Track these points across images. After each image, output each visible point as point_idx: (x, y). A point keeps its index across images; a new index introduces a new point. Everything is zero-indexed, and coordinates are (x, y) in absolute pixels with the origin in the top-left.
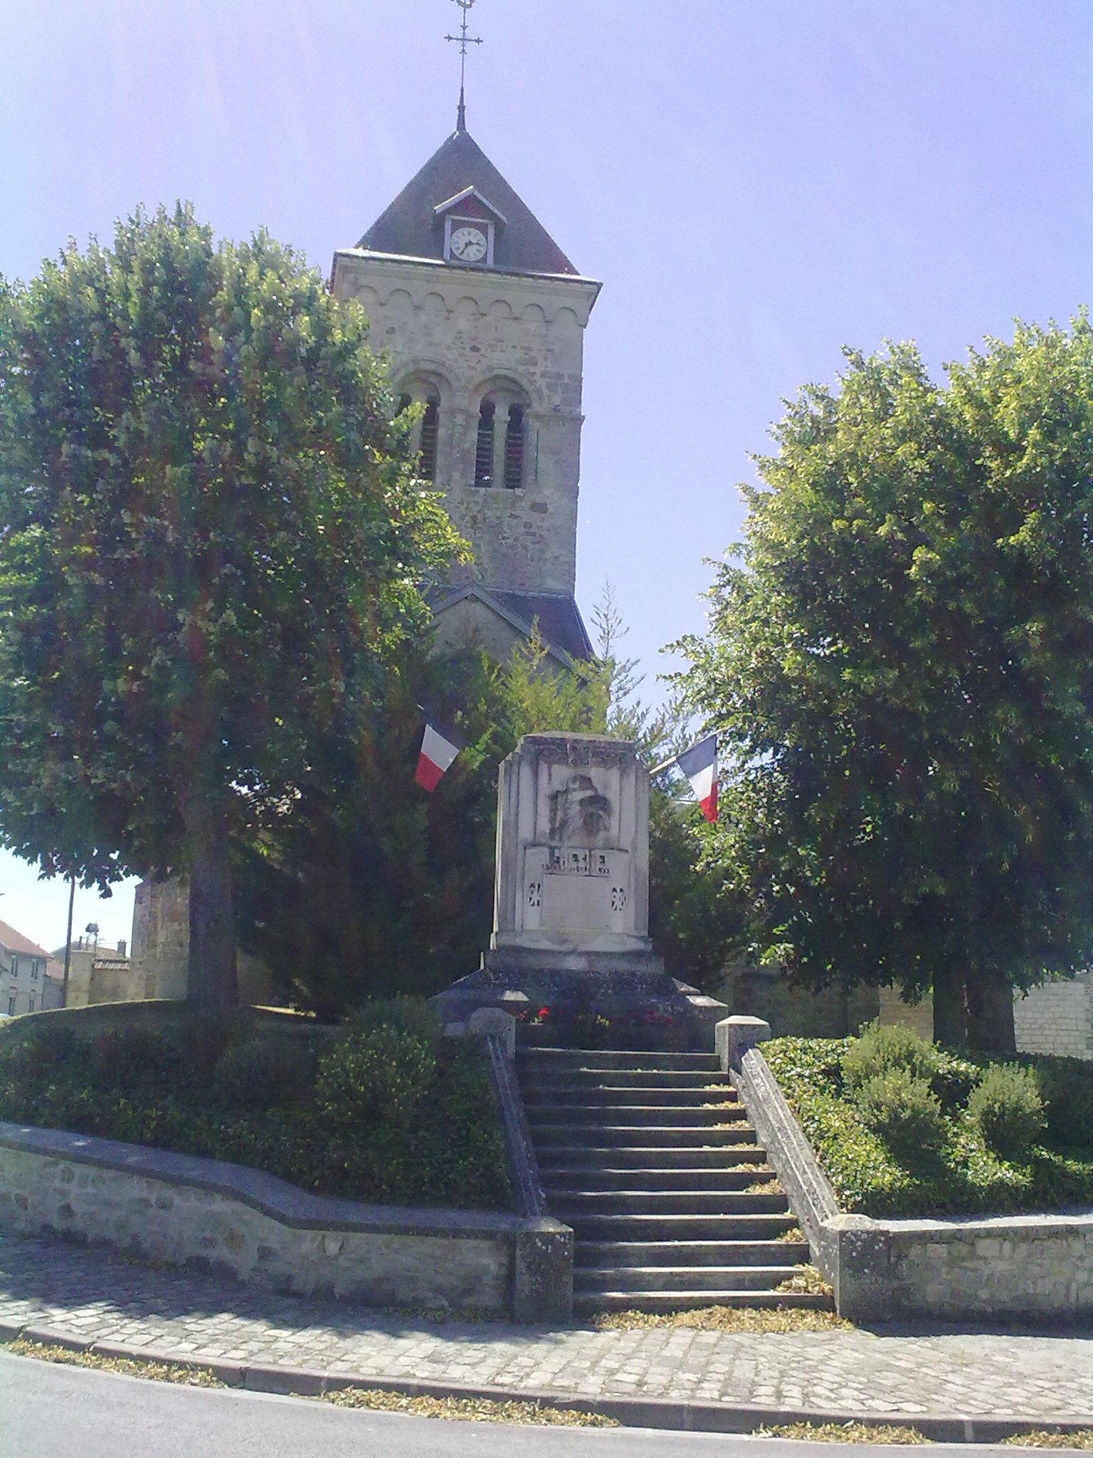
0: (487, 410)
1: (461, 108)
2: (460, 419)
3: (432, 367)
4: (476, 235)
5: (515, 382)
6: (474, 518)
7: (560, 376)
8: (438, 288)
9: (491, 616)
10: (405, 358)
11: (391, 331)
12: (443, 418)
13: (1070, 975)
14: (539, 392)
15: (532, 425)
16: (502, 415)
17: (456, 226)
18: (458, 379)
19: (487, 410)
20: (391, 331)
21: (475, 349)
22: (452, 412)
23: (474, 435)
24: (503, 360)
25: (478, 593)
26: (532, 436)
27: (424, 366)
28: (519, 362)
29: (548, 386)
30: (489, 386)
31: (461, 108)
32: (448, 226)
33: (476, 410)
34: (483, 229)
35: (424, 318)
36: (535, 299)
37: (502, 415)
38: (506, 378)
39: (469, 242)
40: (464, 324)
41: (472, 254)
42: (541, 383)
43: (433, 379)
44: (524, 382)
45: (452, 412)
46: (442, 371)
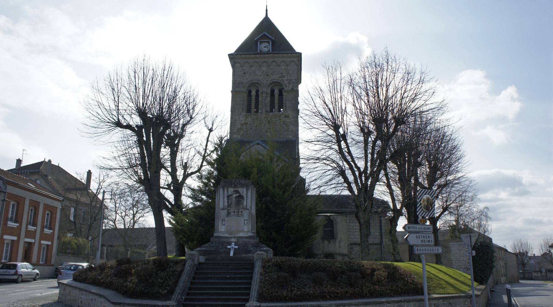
0: (272, 92)
1: (267, 10)
2: (264, 95)
3: (256, 81)
4: (267, 44)
5: (279, 83)
6: (269, 122)
7: (292, 80)
8: (256, 60)
9: (264, 148)
10: (249, 80)
11: (245, 73)
12: (260, 95)
13: (490, 240)
14: (286, 84)
15: (284, 93)
16: (277, 92)
17: (261, 43)
18: (263, 84)
19: (272, 92)
20: (245, 73)
21: (268, 75)
22: (262, 93)
23: (269, 99)
24: (276, 77)
25: (259, 142)
26: (284, 97)
27: (254, 81)
28: (280, 77)
29: (288, 83)
30: (273, 85)
31: (267, 10)
32: (259, 43)
33: (269, 92)
34: (268, 42)
35: (253, 69)
36: (283, 59)
37: (277, 92)
38: (276, 82)
39: (264, 47)
40: (264, 69)
41: (266, 50)
42: (286, 82)
43: (257, 85)
44: (282, 82)
45: (262, 93)
46: (259, 82)
